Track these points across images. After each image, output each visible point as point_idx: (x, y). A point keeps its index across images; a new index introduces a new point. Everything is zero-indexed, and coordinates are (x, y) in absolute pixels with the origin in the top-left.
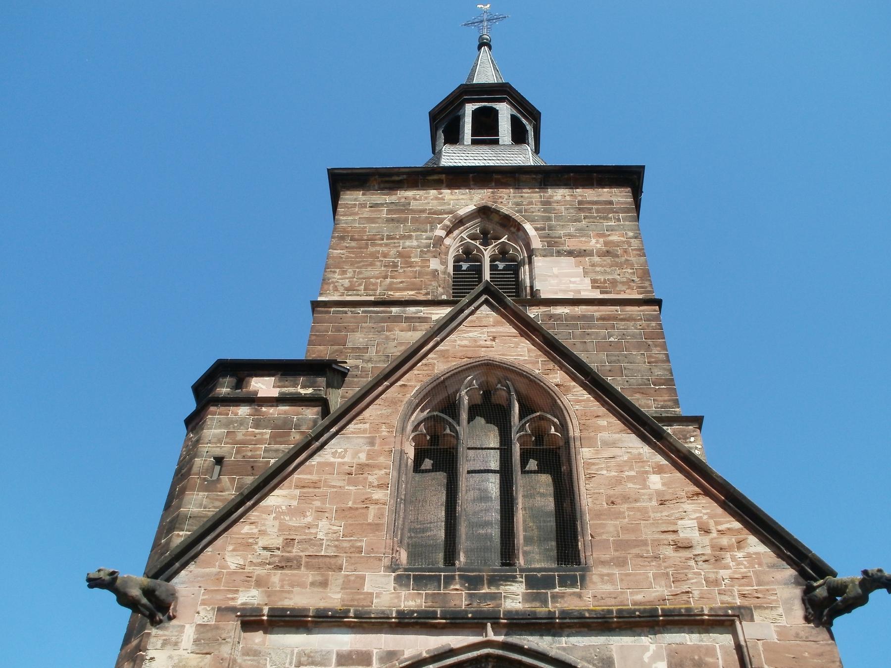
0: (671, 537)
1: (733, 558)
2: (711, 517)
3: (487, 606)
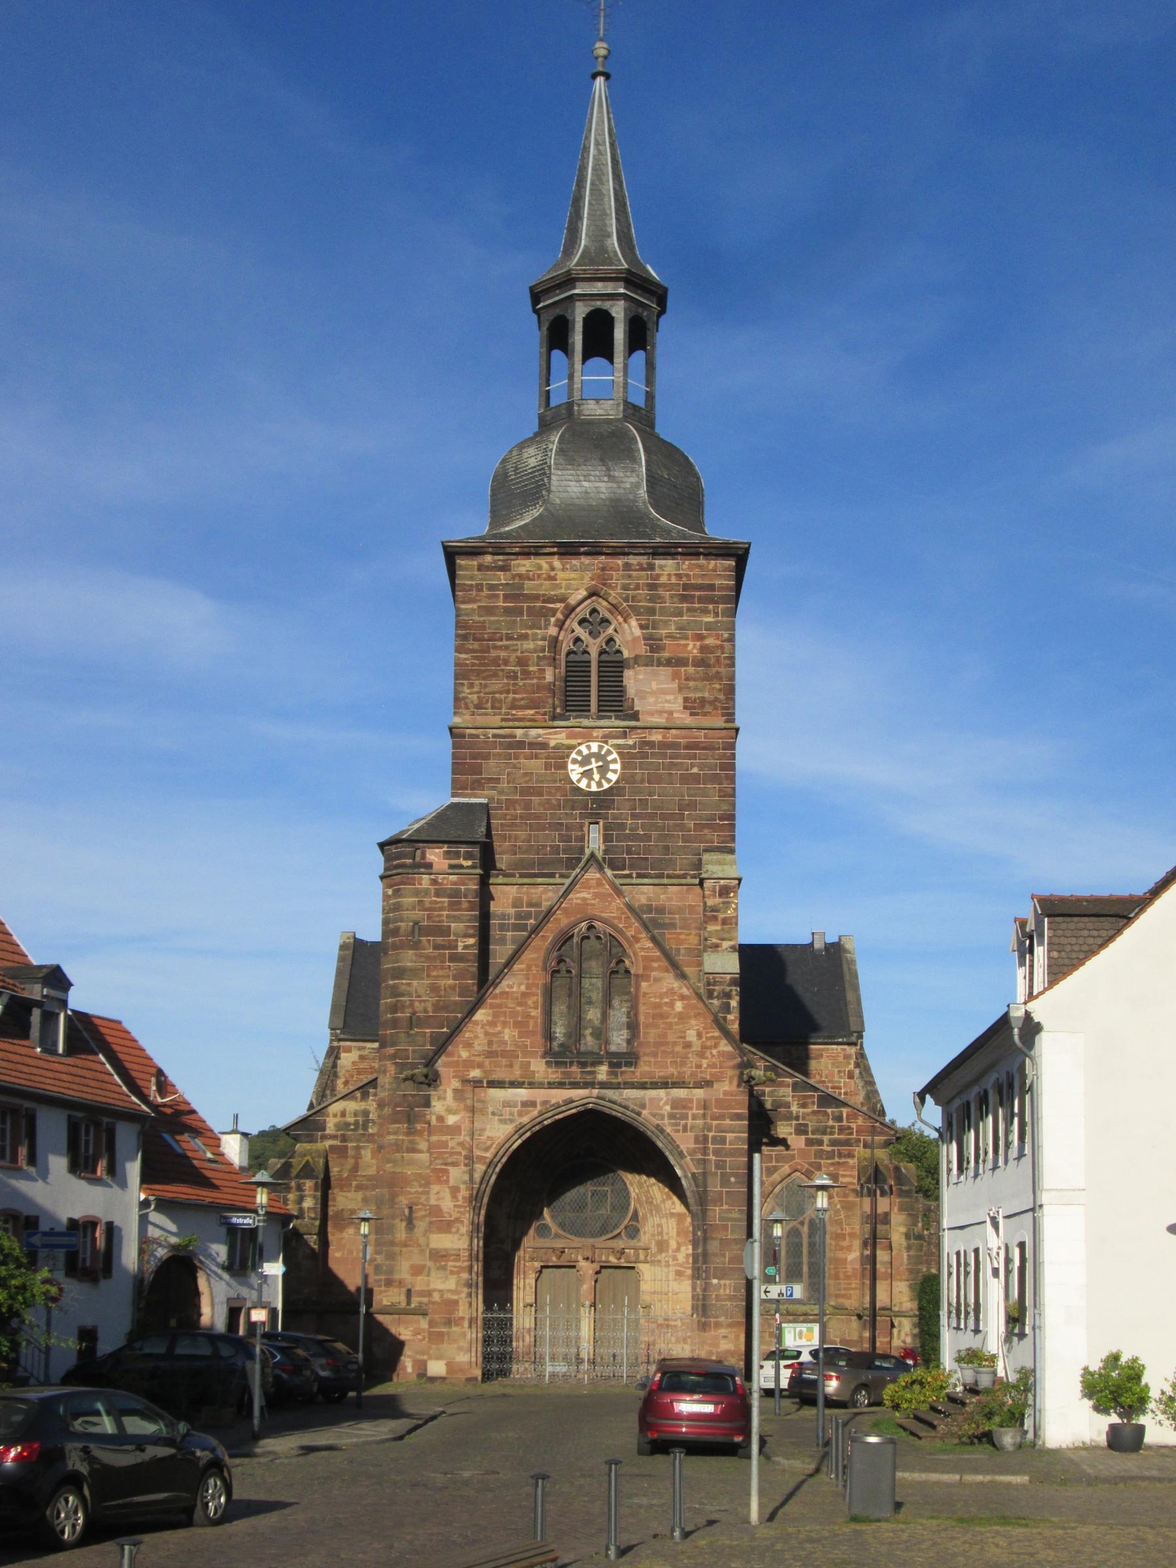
2: (704, 1028)
3: (589, 1078)
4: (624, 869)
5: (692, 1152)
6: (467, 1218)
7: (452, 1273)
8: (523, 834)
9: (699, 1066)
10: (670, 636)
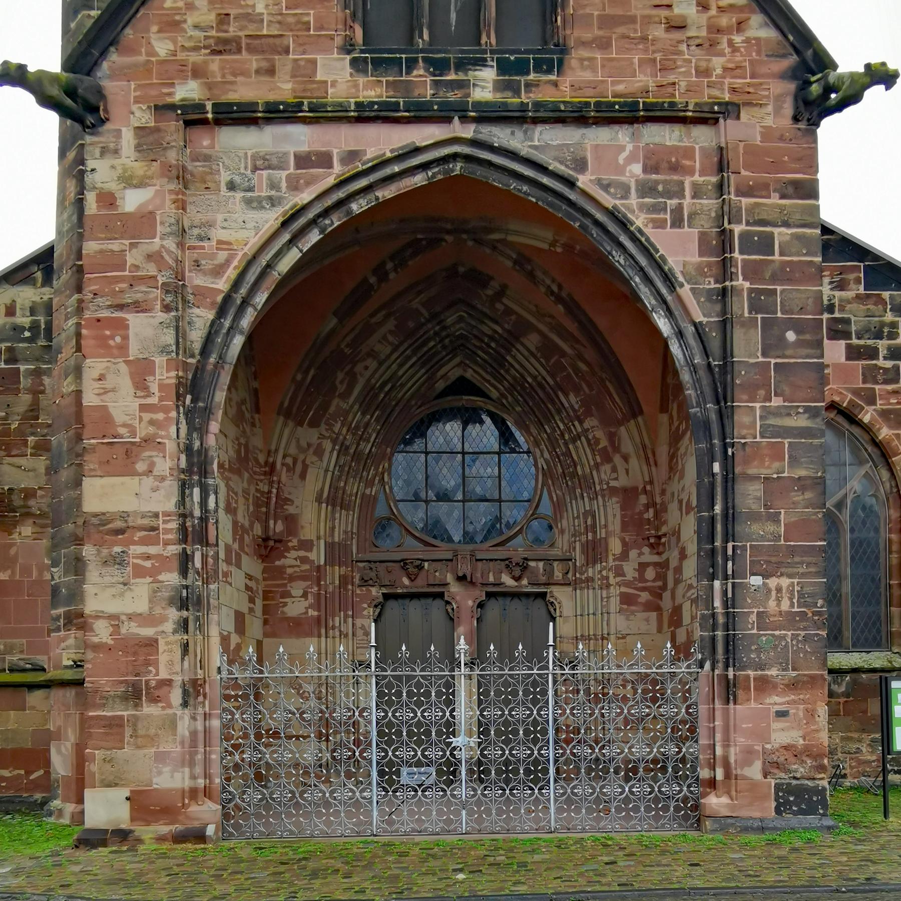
0: (664, 13)
1: (730, 43)
3: (453, 96)
6: (172, 435)
7: (140, 572)
9: (704, 72)
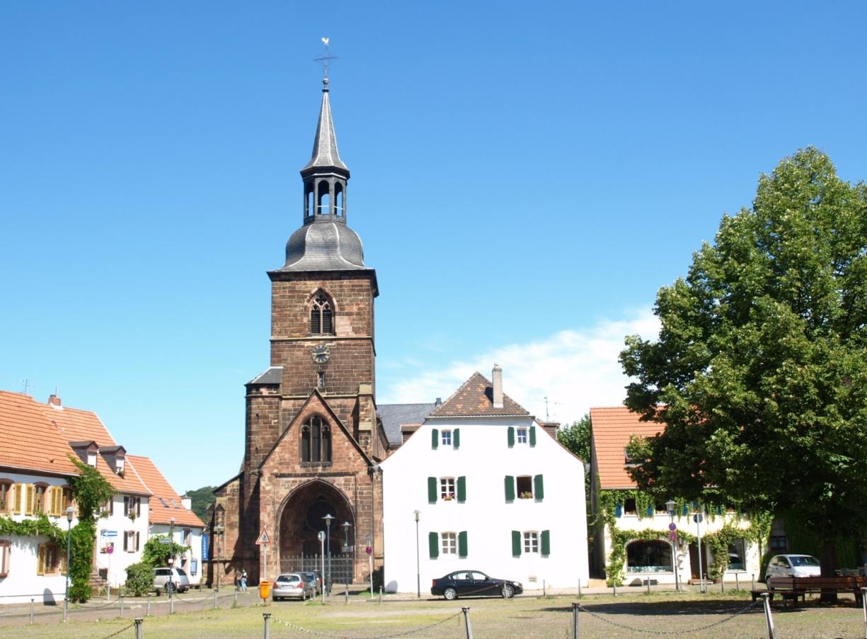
3: (316, 472)
4: (331, 391)
5: (352, 498)
6: (273, 524)
8: (296, 380)
10: (347, 304)
